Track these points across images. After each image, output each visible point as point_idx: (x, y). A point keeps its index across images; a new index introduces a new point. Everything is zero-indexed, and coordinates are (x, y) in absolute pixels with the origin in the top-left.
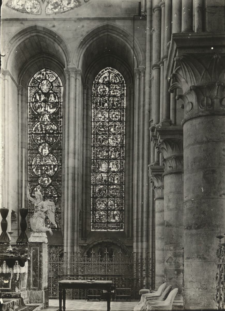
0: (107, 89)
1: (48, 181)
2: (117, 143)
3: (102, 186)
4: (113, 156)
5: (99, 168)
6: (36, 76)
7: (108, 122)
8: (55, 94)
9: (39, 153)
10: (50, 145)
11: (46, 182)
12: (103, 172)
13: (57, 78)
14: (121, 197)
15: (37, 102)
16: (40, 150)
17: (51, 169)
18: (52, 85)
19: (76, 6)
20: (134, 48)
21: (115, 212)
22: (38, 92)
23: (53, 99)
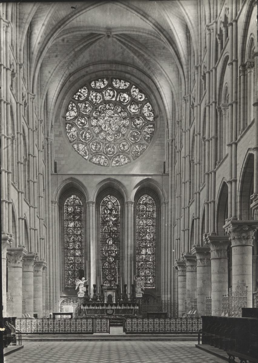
0: (145, 207)
1: (112, 259)
2: (151, 238)
3: (142, 263)
4: (148, 246)
5: (141, 252)
6: (105, 199)
7: (146, 226)
8: (116, 210)
9: (107, 243)
10: (113, 239)
11: (111, 260)
12: (143, 254)
13: (116, 201)
14: (153, 269)
15: (105, 214)
16: (107, 242)
17: (114, 253)
18: (114, 204)
19: (128, 162)
20: (162, 191)
21: (150, 277)
22: (106, 209)
23: (114, 212)
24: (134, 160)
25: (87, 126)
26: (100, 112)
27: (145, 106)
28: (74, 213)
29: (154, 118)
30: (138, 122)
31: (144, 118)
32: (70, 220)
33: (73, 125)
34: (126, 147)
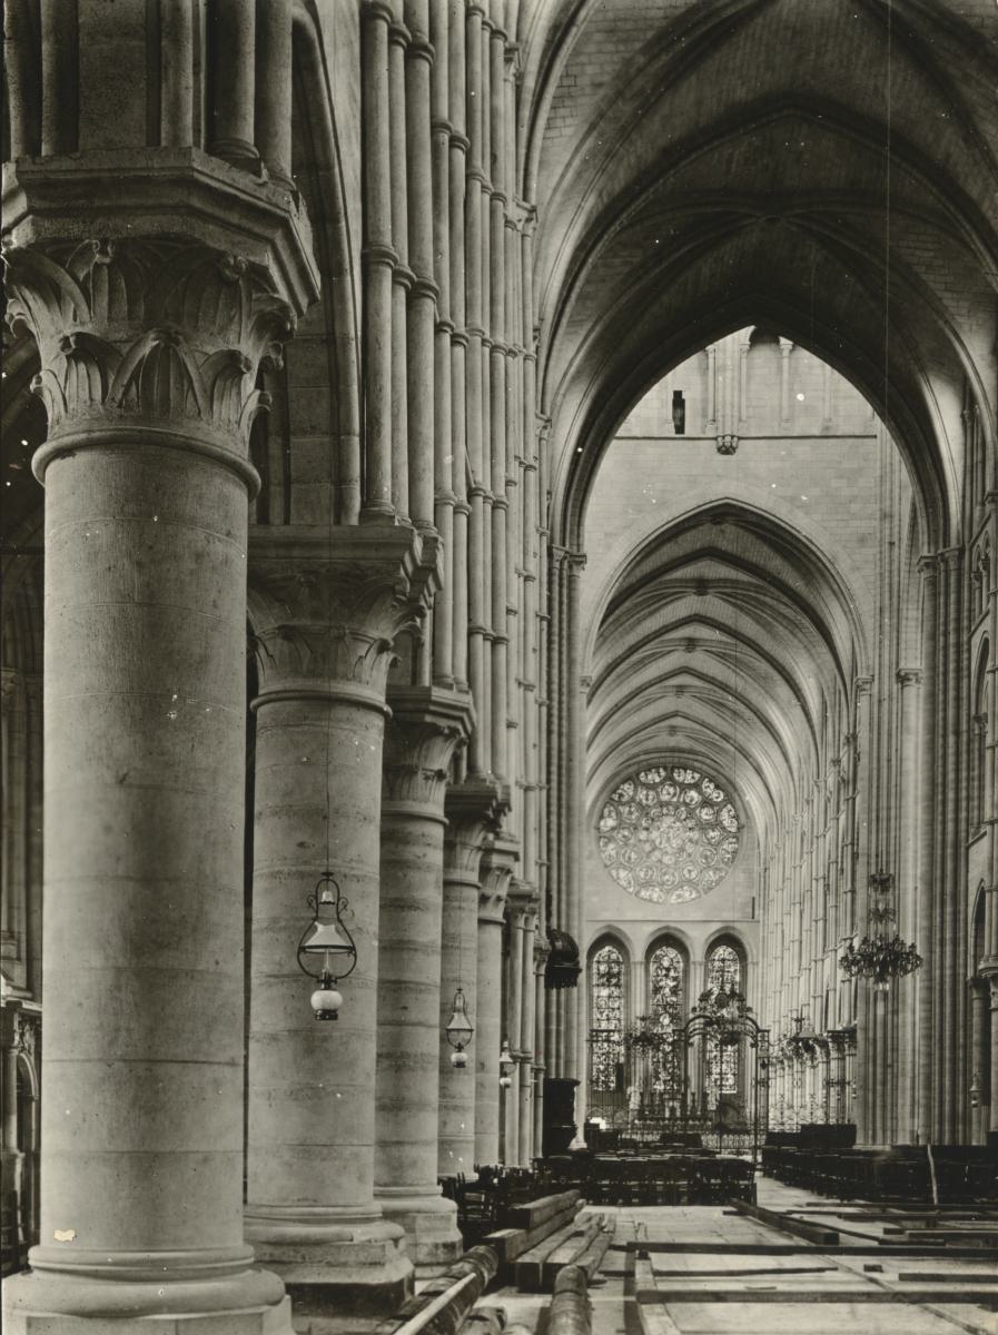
6: (658, 952)
8: (675, 969)
10: (671, 1015)
15: (658, 976)
19: (696, 898)
24: (706, 893)
25: (632, 841)
26: (653, 820)
27: (725, 810)
28: (609, 975)
29: (738, 829)
30: (712, 834)
31: (724, 828)
32: (603, 985)
33: (610, 840)
34: (693, 875)
